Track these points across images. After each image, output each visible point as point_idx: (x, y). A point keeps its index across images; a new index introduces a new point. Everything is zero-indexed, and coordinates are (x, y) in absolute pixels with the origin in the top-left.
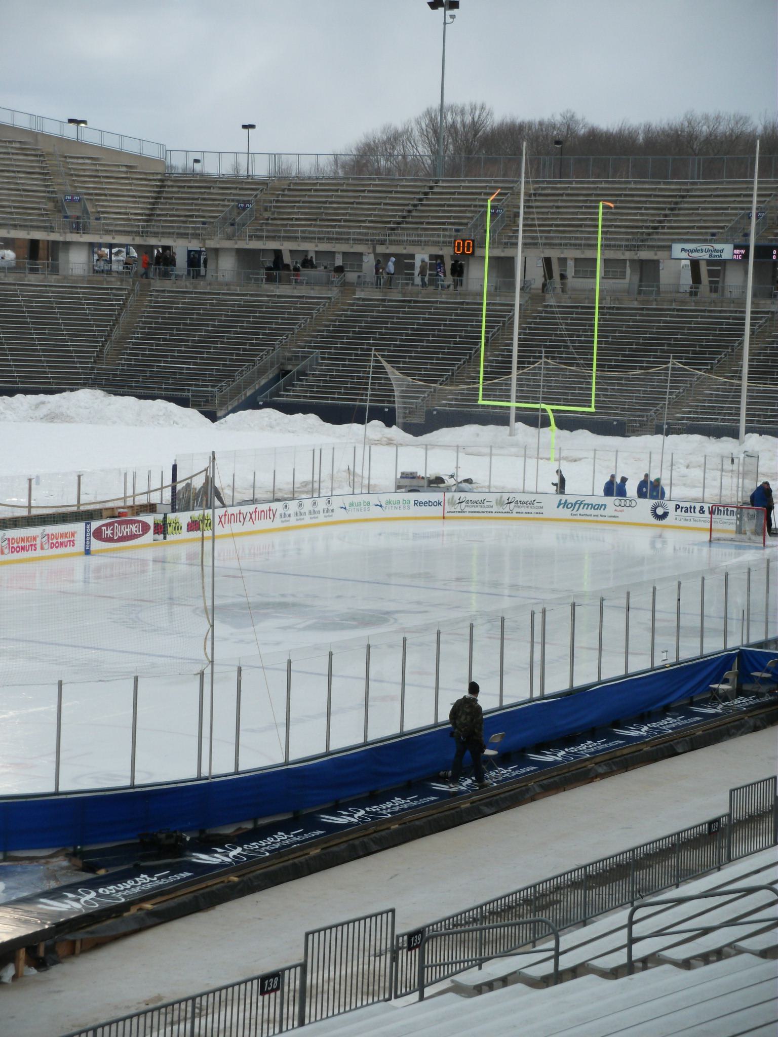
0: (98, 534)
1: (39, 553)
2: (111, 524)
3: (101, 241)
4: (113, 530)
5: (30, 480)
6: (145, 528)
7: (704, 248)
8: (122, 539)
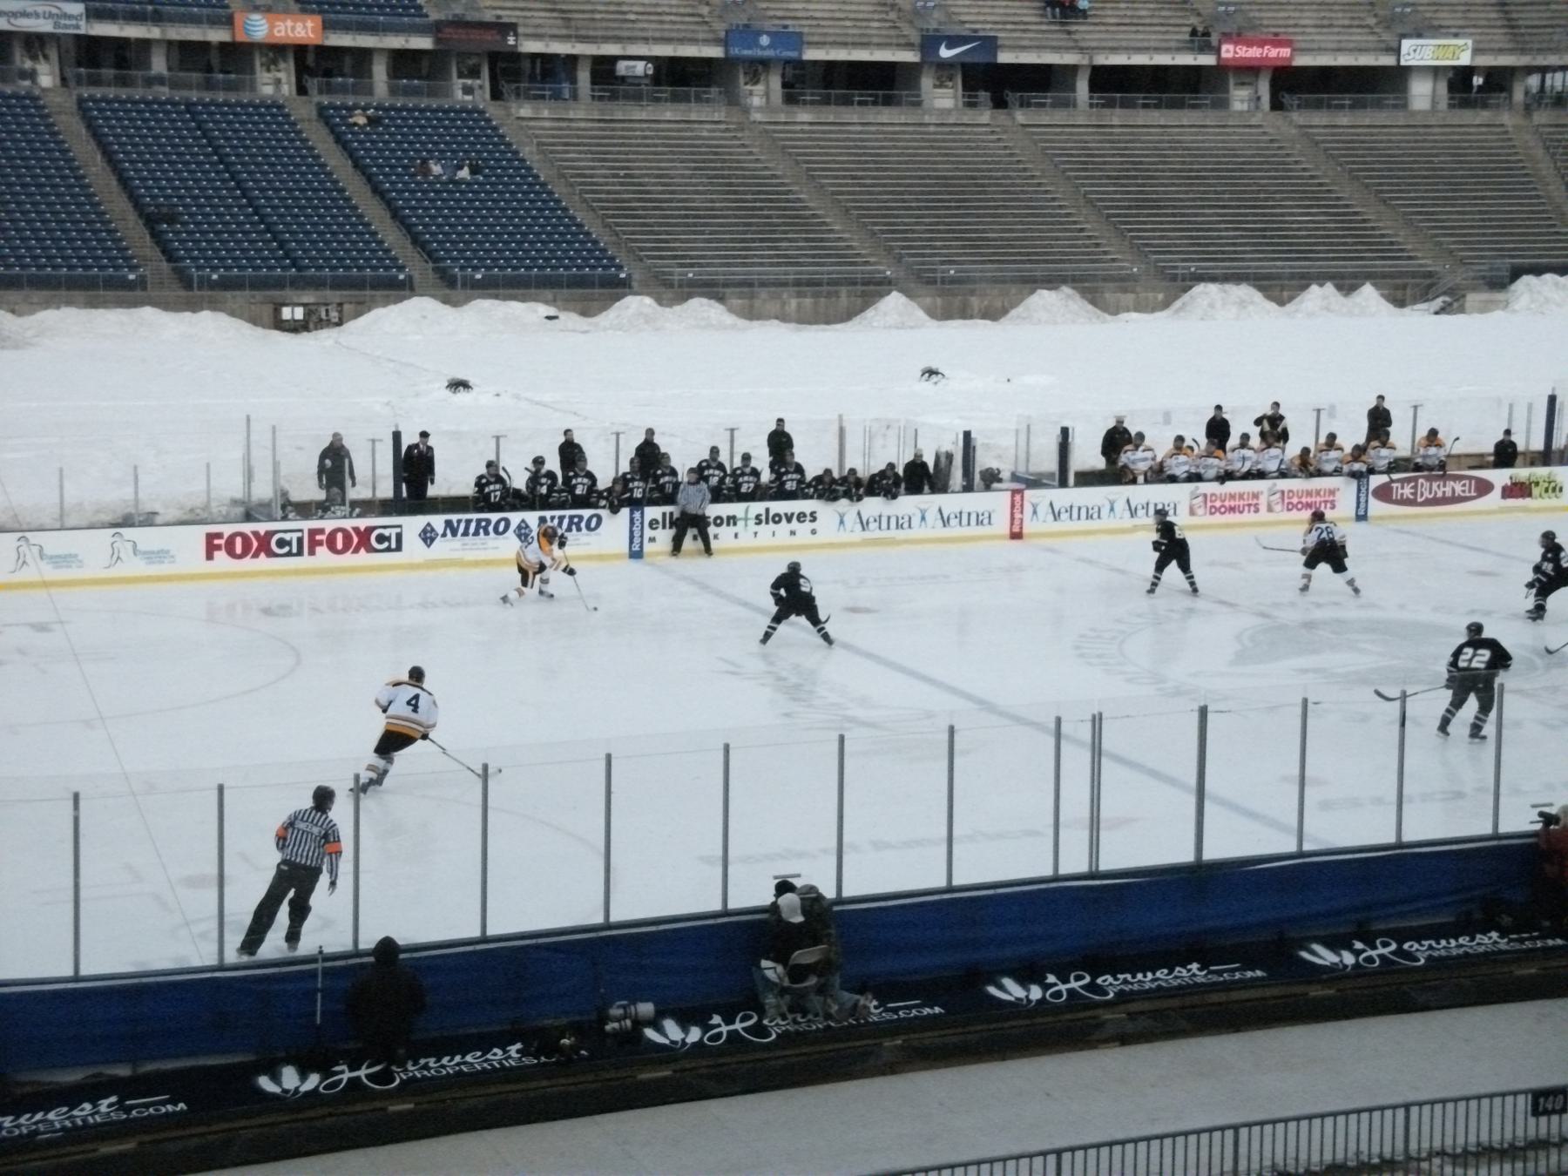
0: (1384, 493)
1: (1263, 515)
2: (1415, 479)
3: (1545, 63)
4: (1415, 487)
5: (1319, 411)
6: (1484, 488)
7: (40, 9)
8: (1445, 501)
